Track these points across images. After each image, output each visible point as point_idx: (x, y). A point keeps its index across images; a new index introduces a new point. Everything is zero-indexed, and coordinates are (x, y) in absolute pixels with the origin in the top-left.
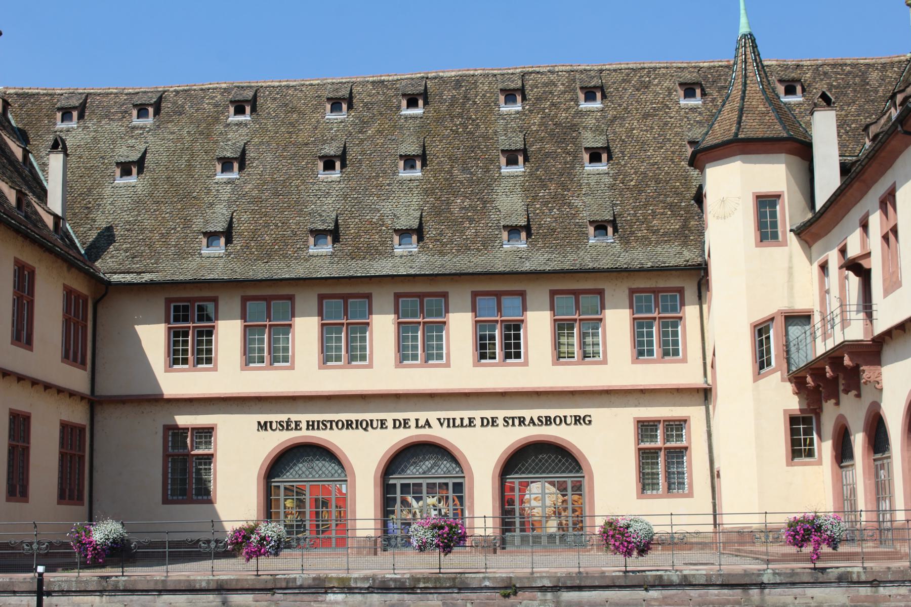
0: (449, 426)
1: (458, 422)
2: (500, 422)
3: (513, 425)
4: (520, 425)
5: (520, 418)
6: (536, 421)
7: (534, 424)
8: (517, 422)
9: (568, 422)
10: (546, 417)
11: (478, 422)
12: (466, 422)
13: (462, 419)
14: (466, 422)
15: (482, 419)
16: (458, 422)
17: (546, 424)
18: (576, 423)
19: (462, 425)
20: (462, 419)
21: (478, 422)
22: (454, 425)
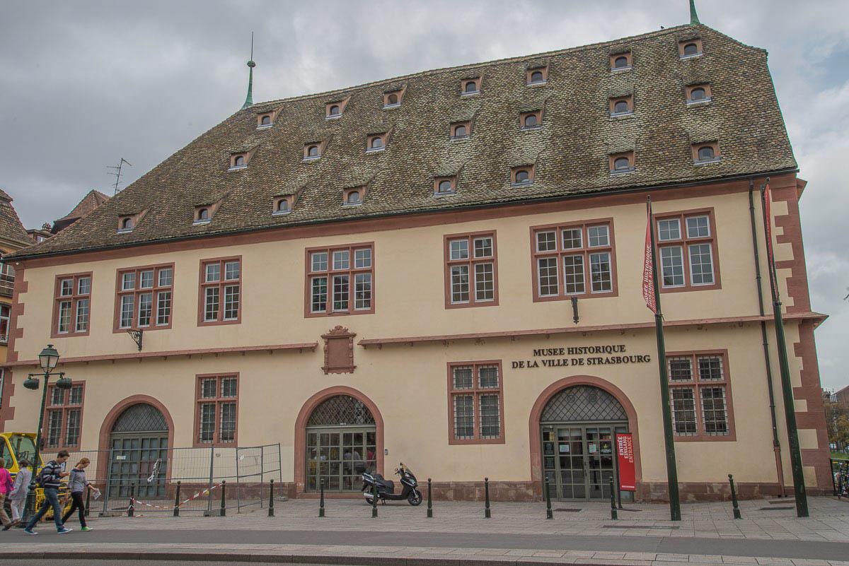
0: (550, 365)
1: (556, 363)
2: (585, 361)
3: (594, 363)
4: (599, 363)
5: (599, 359)
6: (610, 361)
7: (609, 363)
8: (597, 361)
9: (634, 360)
10: (617, 358)
11: (570, 362)
12: (562, 362)
13: (559, 360)
14: (562, 362)
15: (573, 360)
16: (556, 363)
17: (617, 362)
18: (638, 361)
19: (559, 365)
20: (559, 360)
21: (570, 362)
22: (553, 365)
